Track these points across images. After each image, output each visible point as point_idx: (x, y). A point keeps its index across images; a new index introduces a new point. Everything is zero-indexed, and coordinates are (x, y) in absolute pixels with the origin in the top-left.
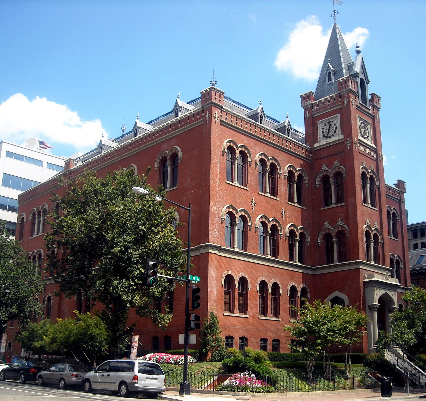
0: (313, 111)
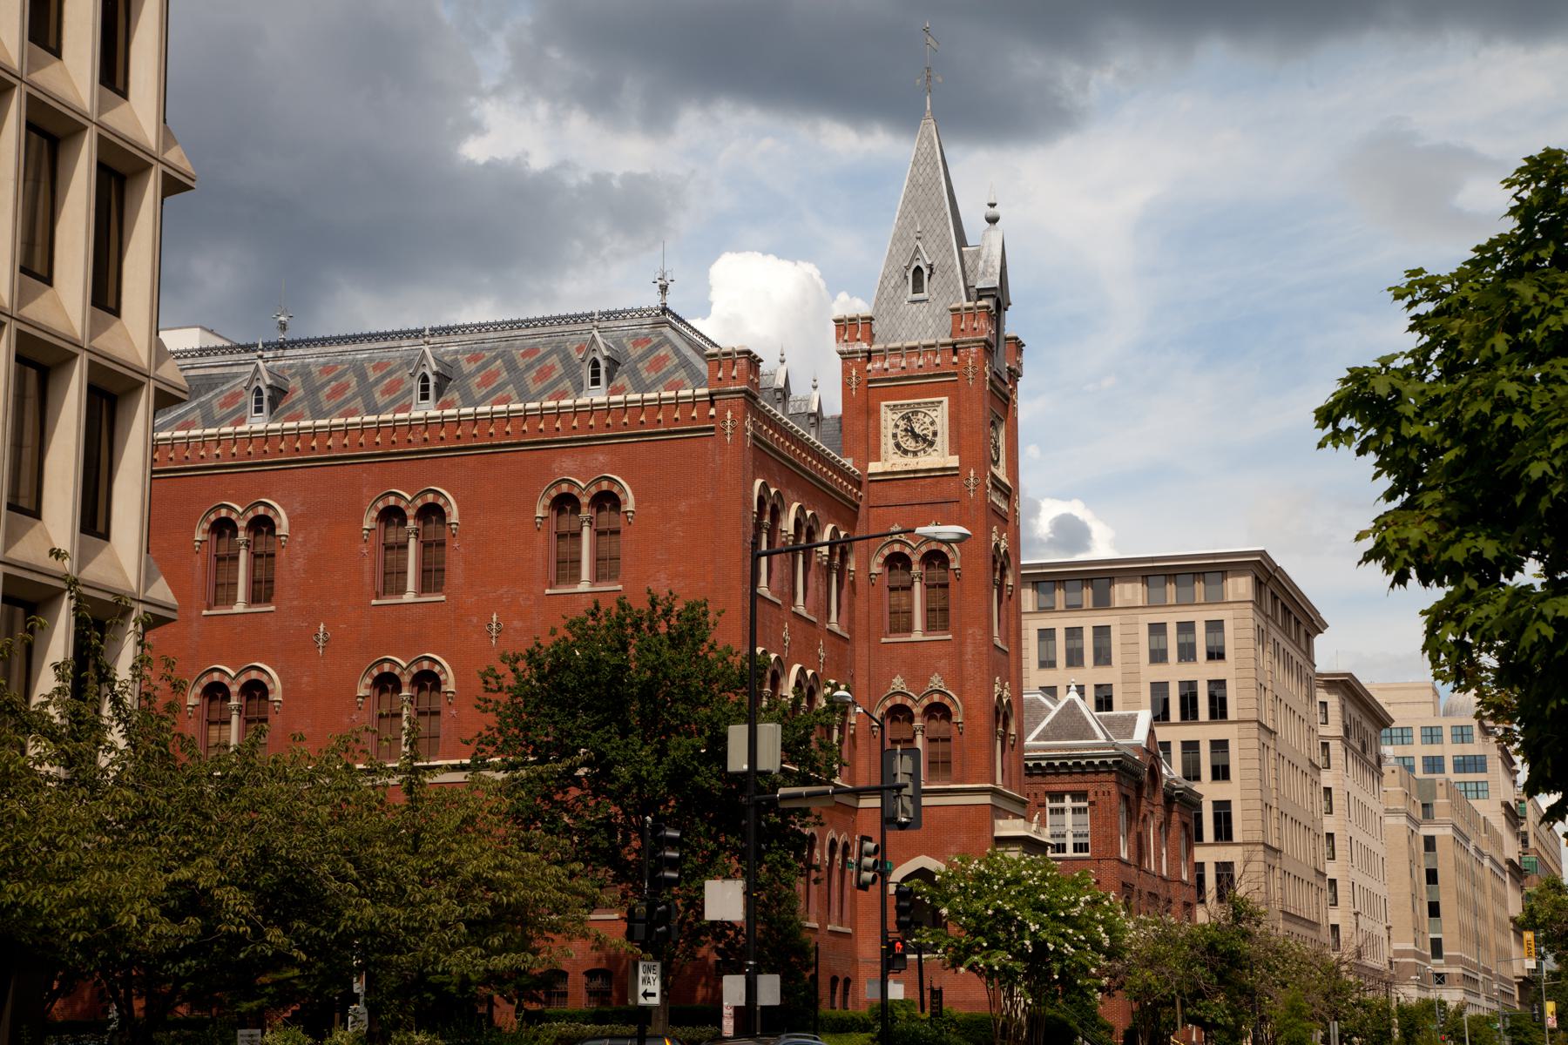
0: (869, 371)
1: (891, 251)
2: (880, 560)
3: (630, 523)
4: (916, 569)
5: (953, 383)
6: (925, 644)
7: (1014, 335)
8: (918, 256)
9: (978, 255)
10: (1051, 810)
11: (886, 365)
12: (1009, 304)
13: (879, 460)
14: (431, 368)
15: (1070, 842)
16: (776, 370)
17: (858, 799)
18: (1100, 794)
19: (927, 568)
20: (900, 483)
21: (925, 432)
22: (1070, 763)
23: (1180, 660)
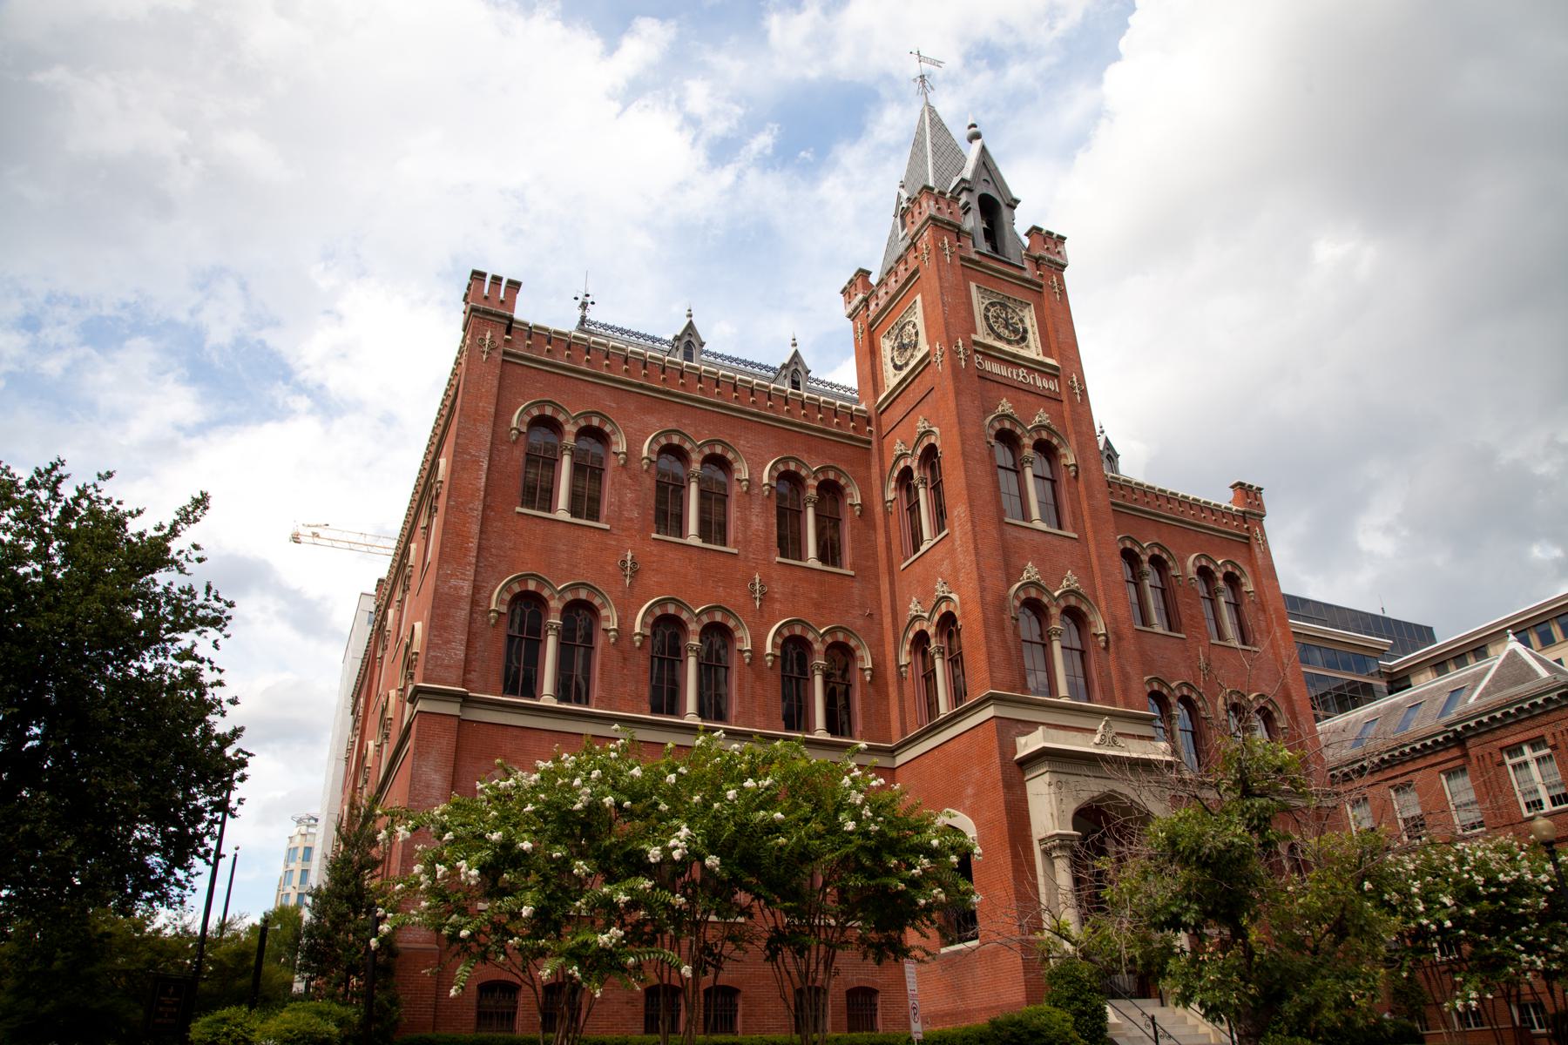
10: (1514, 767)
15: (1544, 796)
18: (1558, 735)
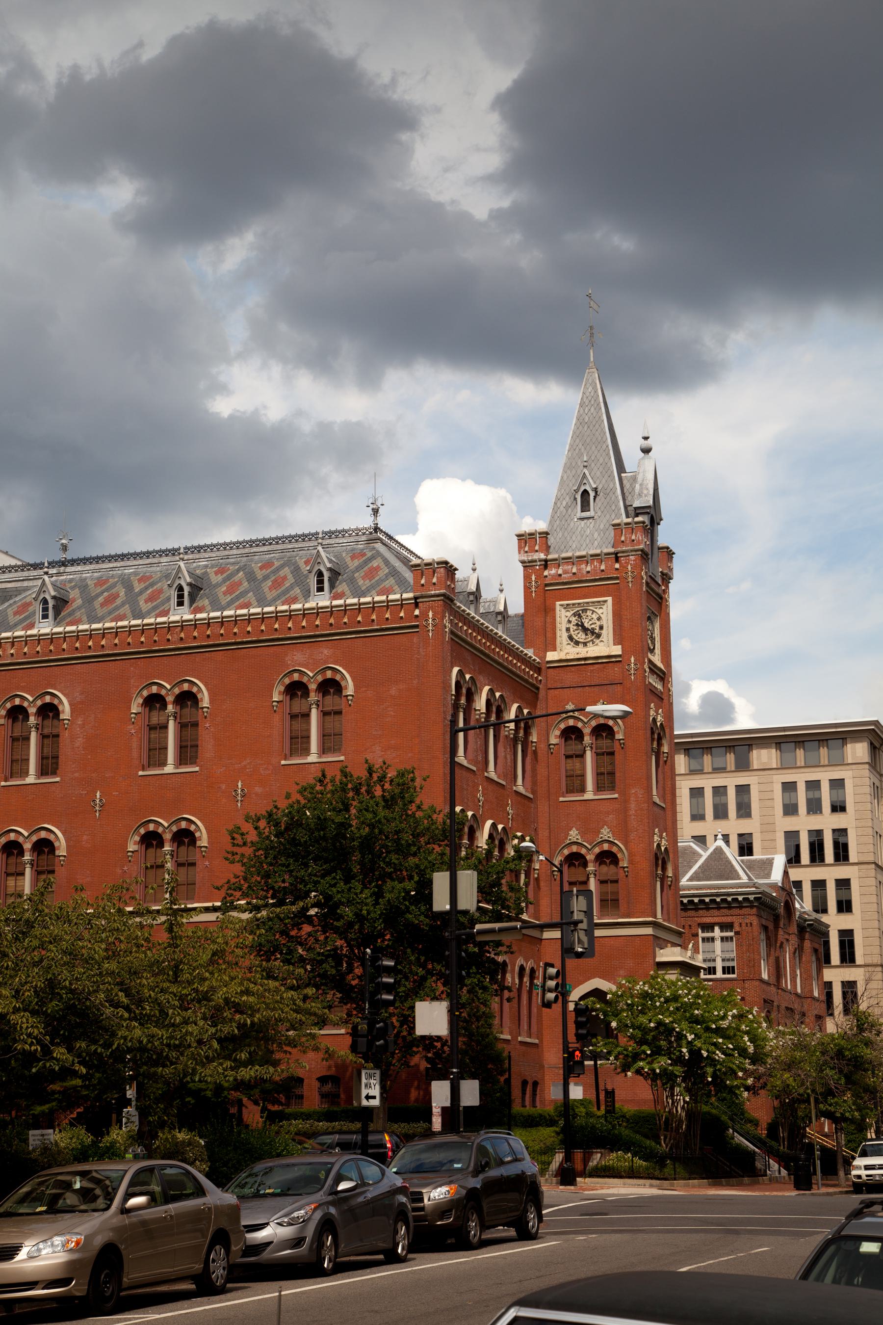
0: (546, 576)
1: (562, 477)
2: (558, 733)
3: (350, 705)
4: (587, 740)
5: (616, 586)
6: (596, 802)
7: (666, 545)
8: (585, 481)
9: (634, 479)
10: (703, 939)
11: (560, 572)
12: (661, 520)
13: (555, 650)
14: (185, 580)
16: (469, 577)
17: (542, 931)
18: (743, 925)
19: (596, 739)
20: (573, 669)
21: (593, 626)
22: (718, 900)
23: (808, 813)
